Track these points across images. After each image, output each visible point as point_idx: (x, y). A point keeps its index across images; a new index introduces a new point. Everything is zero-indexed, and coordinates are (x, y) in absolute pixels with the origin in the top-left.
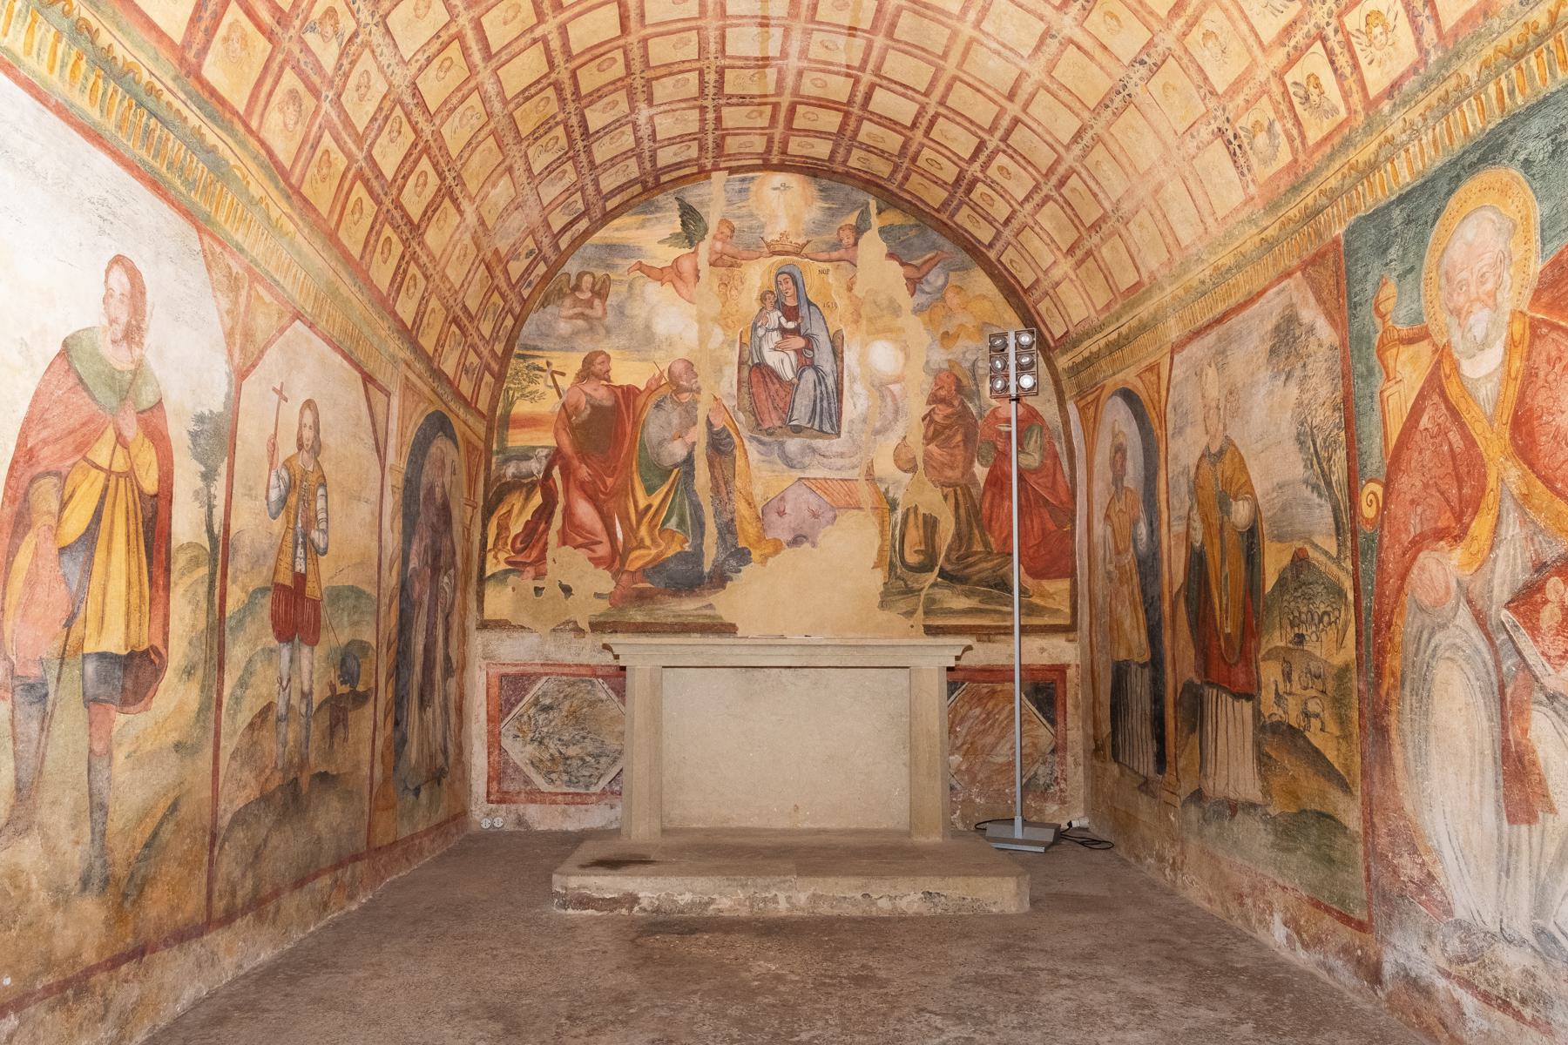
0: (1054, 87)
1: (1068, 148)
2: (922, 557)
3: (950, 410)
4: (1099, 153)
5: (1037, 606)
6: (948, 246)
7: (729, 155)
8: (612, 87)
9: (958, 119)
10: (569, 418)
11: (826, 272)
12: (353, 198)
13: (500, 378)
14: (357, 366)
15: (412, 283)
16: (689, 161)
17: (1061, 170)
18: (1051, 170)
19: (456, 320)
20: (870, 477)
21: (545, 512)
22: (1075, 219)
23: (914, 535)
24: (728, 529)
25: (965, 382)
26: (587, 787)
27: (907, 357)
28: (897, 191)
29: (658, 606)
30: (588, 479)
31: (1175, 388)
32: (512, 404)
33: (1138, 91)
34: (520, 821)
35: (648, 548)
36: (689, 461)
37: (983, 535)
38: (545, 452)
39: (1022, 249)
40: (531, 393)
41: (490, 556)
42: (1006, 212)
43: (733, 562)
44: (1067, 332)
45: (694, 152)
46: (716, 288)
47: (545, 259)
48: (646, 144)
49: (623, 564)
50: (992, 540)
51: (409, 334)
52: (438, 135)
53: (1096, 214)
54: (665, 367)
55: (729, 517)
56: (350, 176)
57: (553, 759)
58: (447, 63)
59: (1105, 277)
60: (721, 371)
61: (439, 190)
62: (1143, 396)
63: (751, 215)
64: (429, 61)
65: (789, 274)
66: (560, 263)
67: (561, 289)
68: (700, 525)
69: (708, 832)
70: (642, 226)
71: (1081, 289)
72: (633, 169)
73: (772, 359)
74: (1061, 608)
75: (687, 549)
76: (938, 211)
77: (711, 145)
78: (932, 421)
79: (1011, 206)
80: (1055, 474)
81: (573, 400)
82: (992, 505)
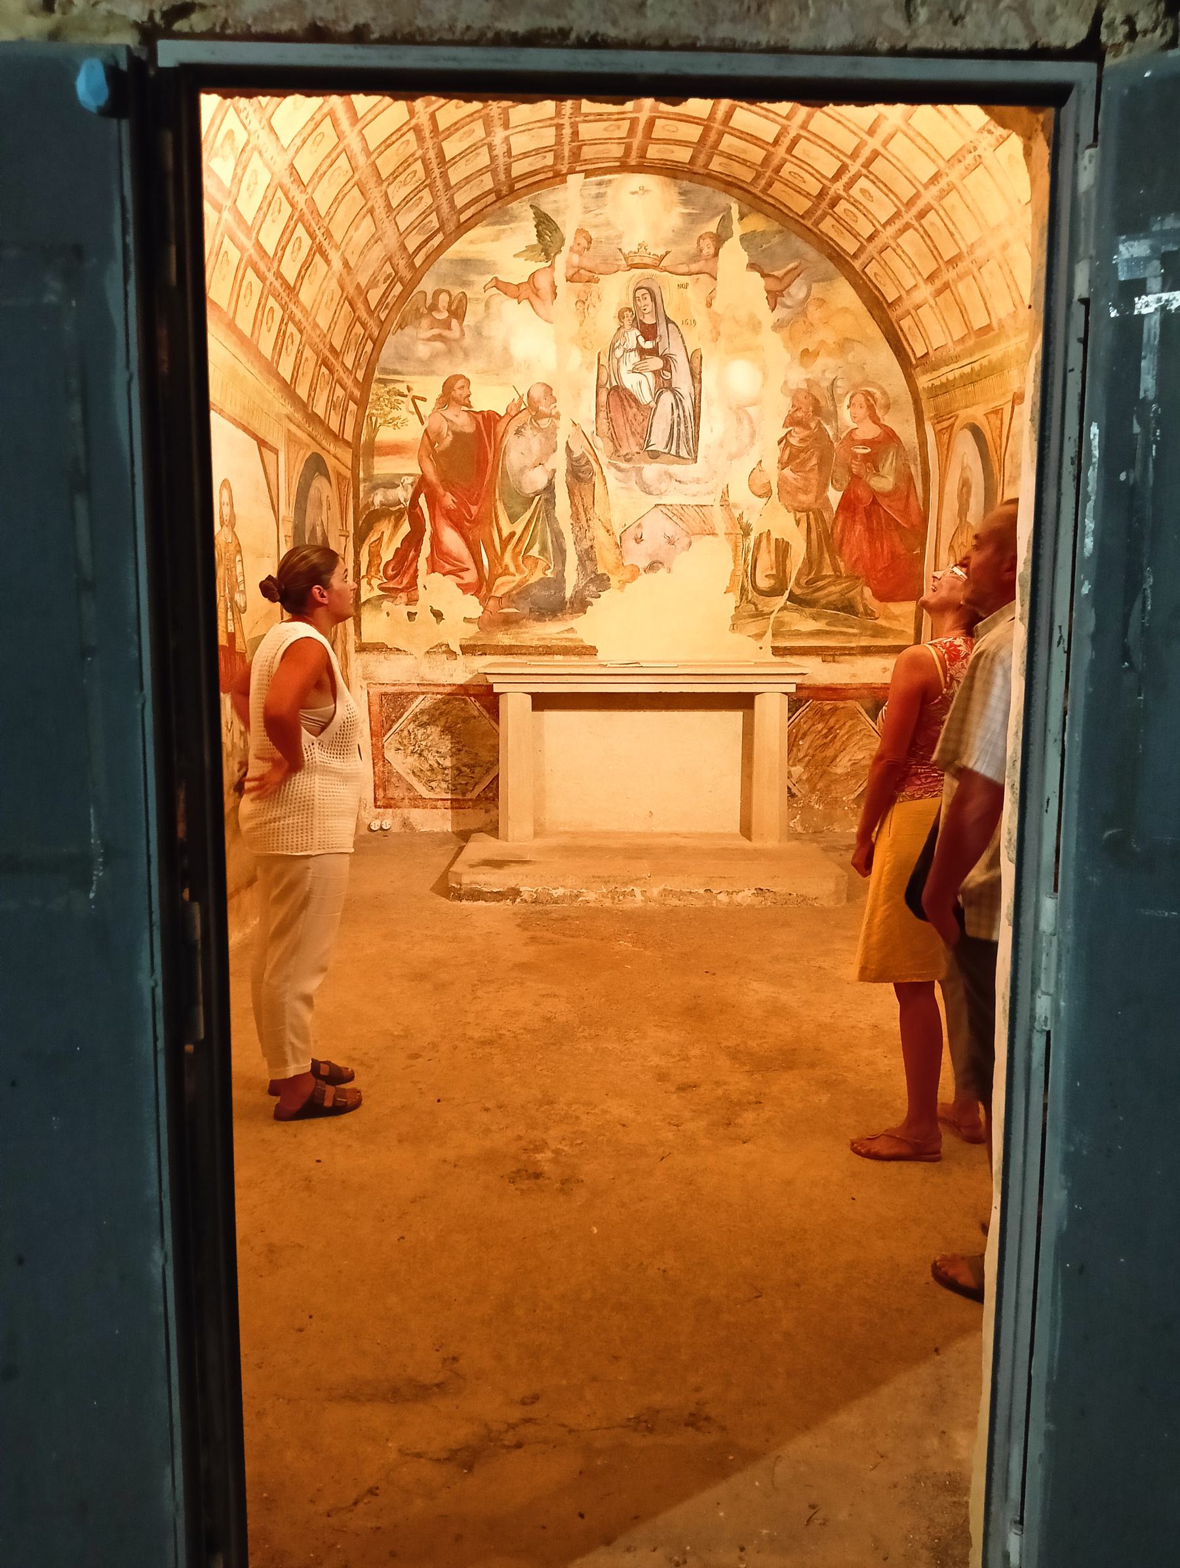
0: (911, 134)
1: (926, 186)
2: (772, 582)
3: (807, 433)
4: (953, 198)
5: (882, 627)
6: (811, 253)
7: (585, 160)
8: (468, 119)
9: (820, 142)
10: (432, 445)
12: (245, 284)
13: (362, 404)
14: (255, 437)
15: (290, 341)
16: (543, 168)
17: (920, 204)
18: (910, 203)
19: (325, 362)
20: (725, 503)
21: (413, 541)
22: (935, 253)
23: (766, 561)
24: (587, 557)
25: (823, 403)
26: (464, 794)
27: (765, 376)
28: (761, 195)
29: (523, 630)
30: (453, 506)
31: (1013, 437)
32: (375, 430)
33: (987, 155)
34: (405, 823)
36: (550, 488)
37: (833, 559)
38: (410, 480)
39: (885, 265)
40: (393, 419)
41: (364, 582)
42: (871, 230)
43: (593, 588)
44: (927, 354)
45: (549, 160)
47: (401, 280)
48: (501, 161)
49: (489, 590)
50: (842, 564)
51: (288, 389)
52: (311, 201)
53: (953, 252)
54: (523, 391)
55: (589, 543)
56: (242, 266)
57: (432, 769)
58: (319, 138)
59: (961, 312)
60: (579, 394)
61: (311, 249)
62: (988, 436)
63: (608, 224)
64: (304, 142)
65: (647, 289)
66: (415, 281)
67: (418, 309)
68: (561, 552)
69: (575, 835)
70: (496, 238)
71: (939, 316)
72: (488, 182)
73: (630, 381)
74: (906, 630)
75: (550, 575)
76: (802, 217)
77: (566, 153)
78: (788, 444)
79: (874, 226)
80: (908, 497)
81: (435, 427)
82: (843, 530)
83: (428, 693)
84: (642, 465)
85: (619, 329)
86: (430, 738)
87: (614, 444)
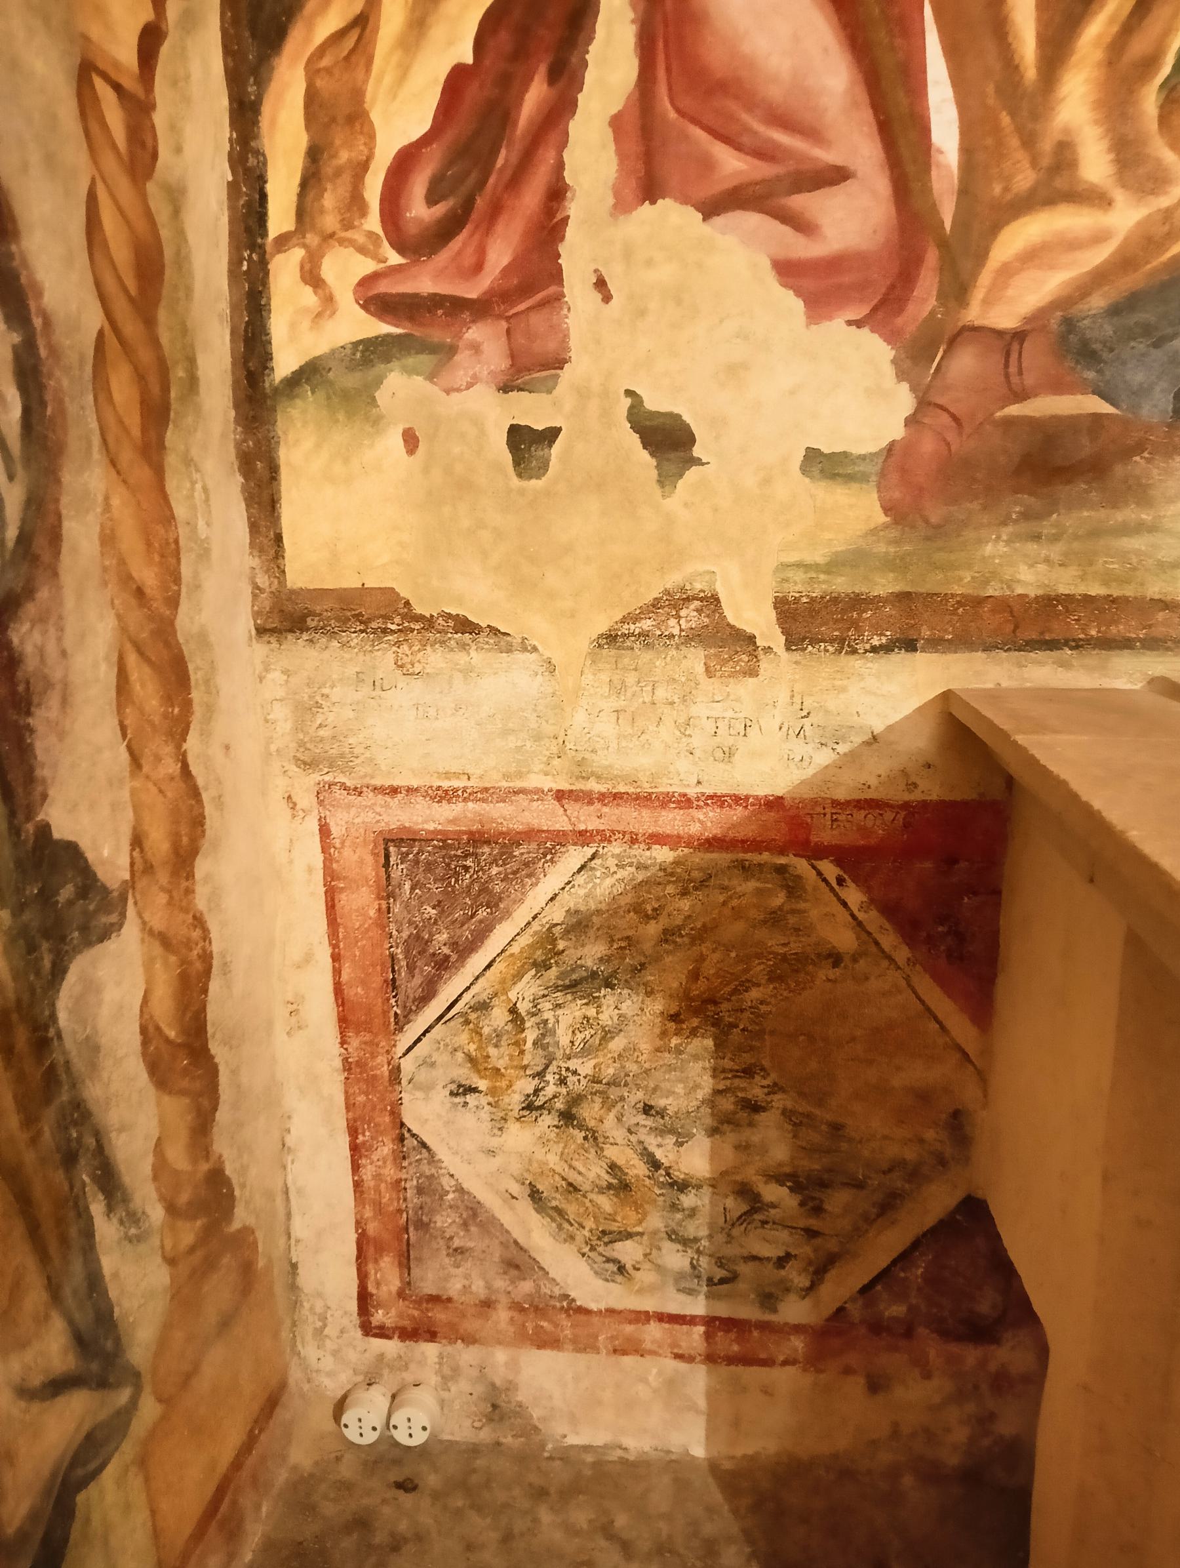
26: (768, 1300)
29: (1128, 514)
35: (1098, 199)
57: (621, 1186)
83: (605, 837)
86: (617, 1044)
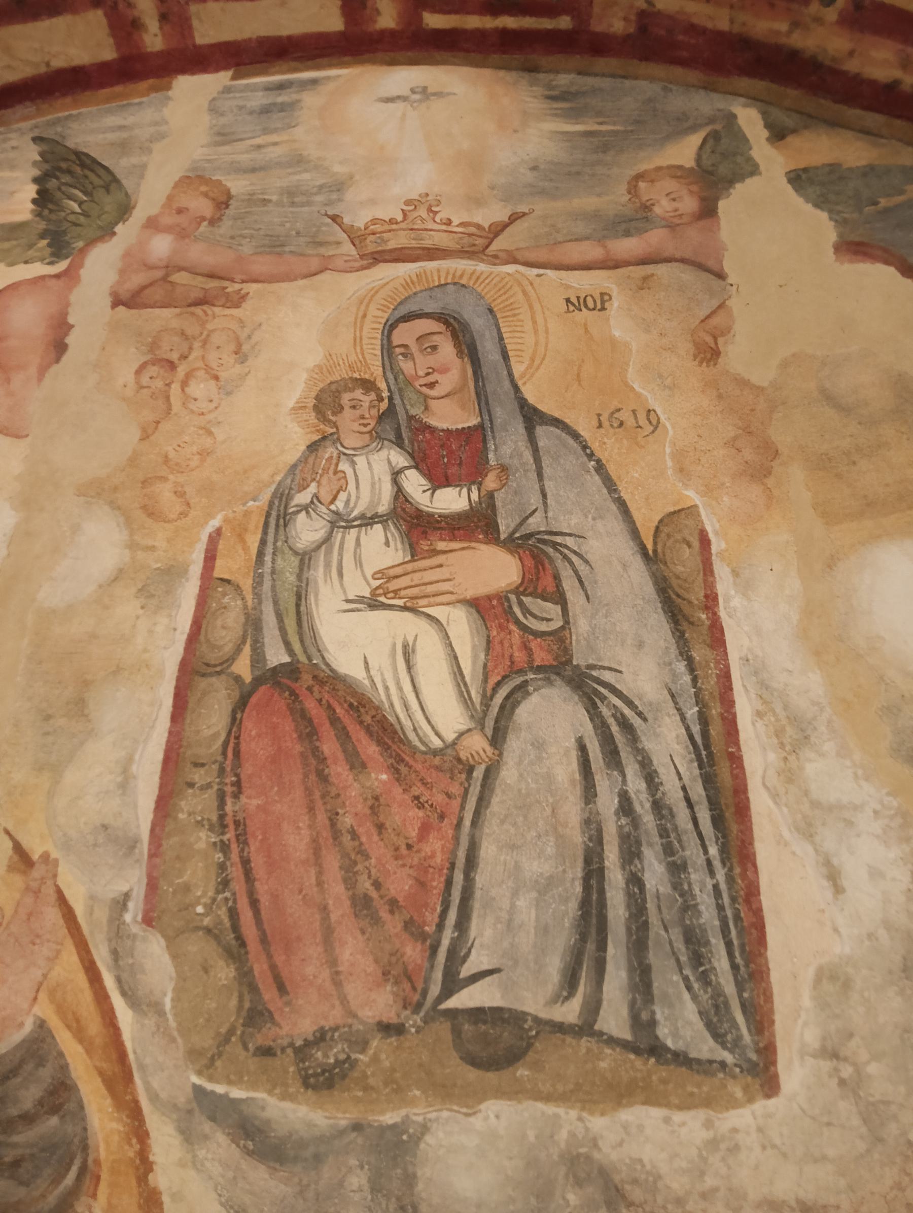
11: (602, 302)
46: (125, 375)
65: (442, 318)
84: (417, 1113)
85: (313, 447)
87: (246, 980)
